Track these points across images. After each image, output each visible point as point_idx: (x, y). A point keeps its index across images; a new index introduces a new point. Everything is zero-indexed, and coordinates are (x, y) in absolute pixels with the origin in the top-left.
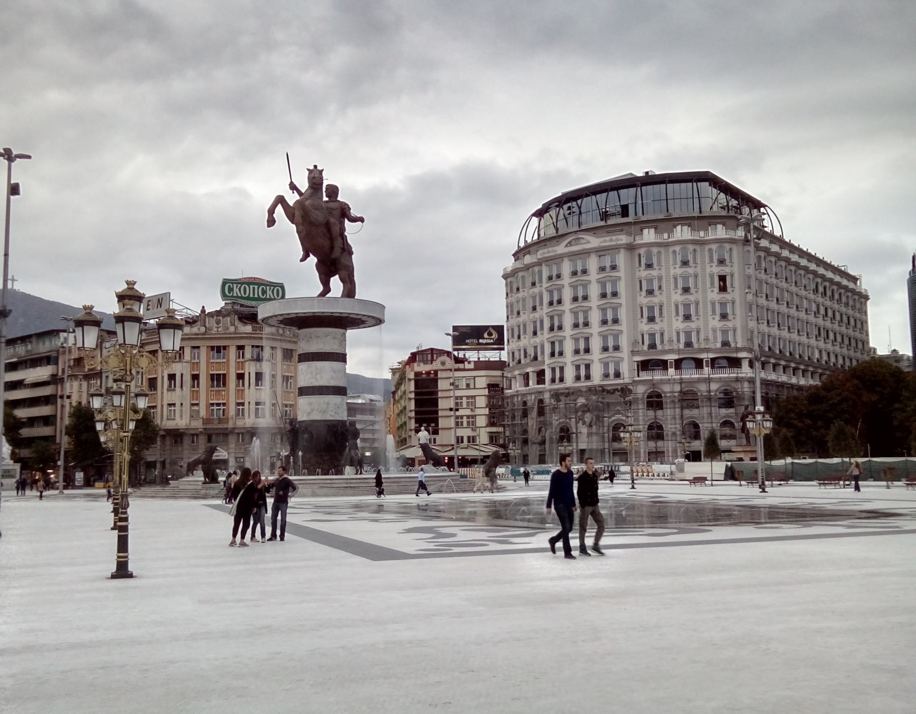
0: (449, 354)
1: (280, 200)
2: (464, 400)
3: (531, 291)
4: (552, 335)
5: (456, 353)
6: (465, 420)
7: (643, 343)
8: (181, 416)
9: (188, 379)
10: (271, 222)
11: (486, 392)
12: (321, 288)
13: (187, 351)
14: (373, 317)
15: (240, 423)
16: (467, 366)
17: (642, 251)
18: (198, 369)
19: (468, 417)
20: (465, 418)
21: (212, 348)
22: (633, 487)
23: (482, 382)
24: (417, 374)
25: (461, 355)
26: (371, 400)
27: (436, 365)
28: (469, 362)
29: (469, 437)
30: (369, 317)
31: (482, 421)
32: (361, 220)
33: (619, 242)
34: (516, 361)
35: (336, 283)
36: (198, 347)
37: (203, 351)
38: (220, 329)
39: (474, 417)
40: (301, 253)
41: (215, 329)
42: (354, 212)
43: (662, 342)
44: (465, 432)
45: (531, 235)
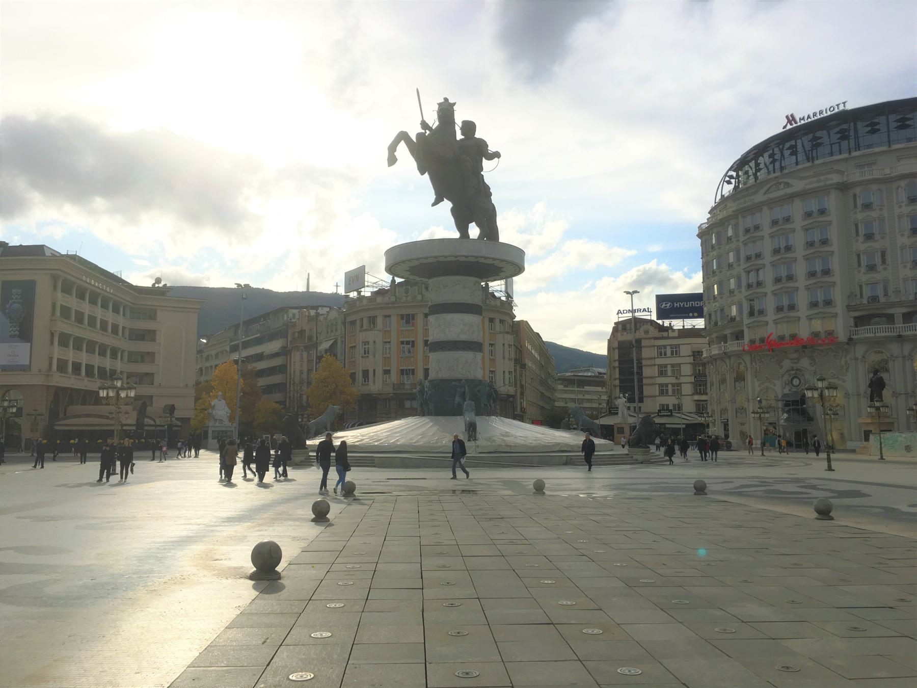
0: (652, 322)
1: (403, 136)
2: (669, 368)
3: (727, 247)
4: (750, 292)
5: (660, 322)
6: (670, 386)
7: (861, 296)
8: (374, 382)
10: (392, 160)
11: (691, 360)
12: (456, 235)
13: (380, 321)
16: (671, 334)
17: (858, 190)
19: (673, 385)
20: (670, 386)
21: (402, 316)
22: (830, 469)
23: (685, 350)
24: (620, 343)
25: (667, 323)
26: (600, 373)
27: (640, 334)
28: (674, 330)
29: (674, 405)
30: (503, 261)
31: (687, 389)
32: (497, 155)
33: (828, 182)
34: (713, 323)
35: (474, 231)
36: (389, 316)
37: (394, 319)
38: (409, 298)
39: (679, 385)
40: (432, 197)
41: (404, 298)
42: (492, 148)
43: (886, 295)
44: (670, 401)
45: (728, 189)
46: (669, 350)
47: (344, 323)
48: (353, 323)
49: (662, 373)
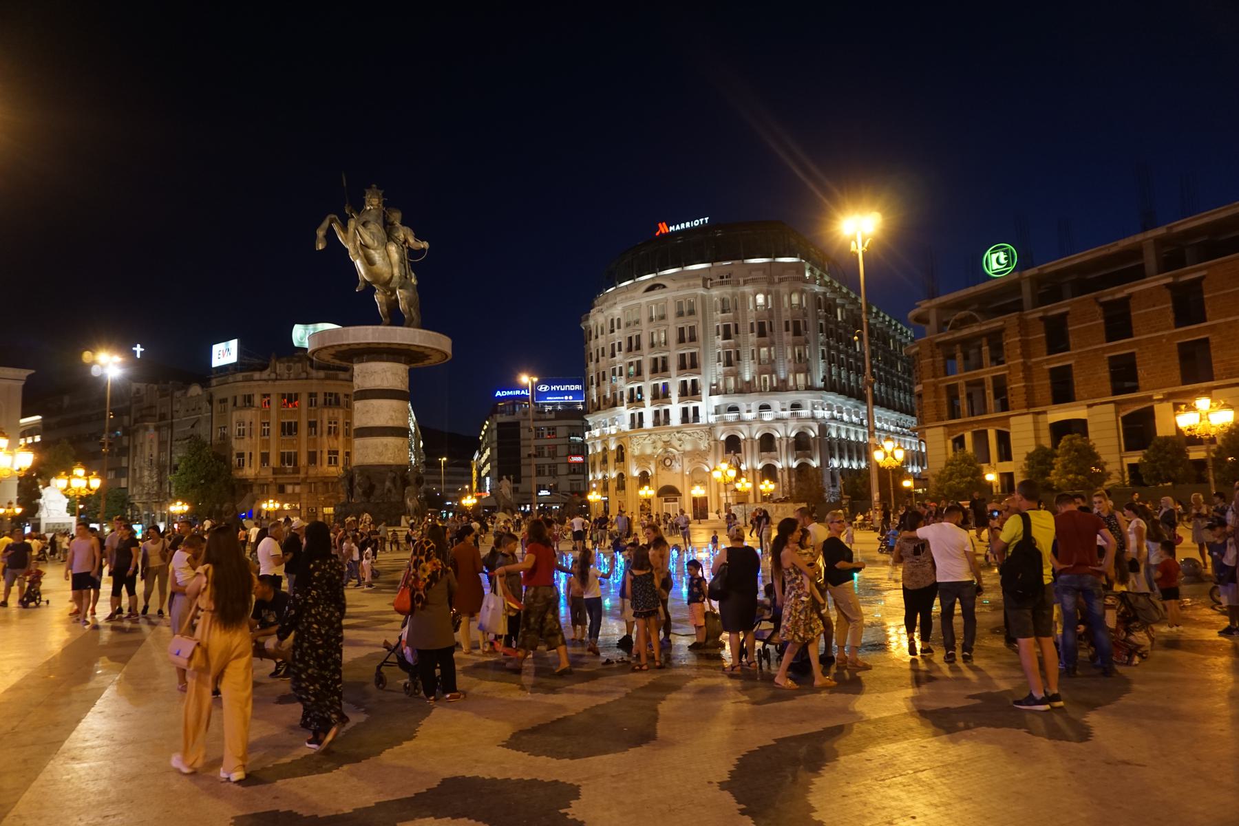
9: (257, 427)
13: (257, 400)
14: (438, 350)
15: (312, 472)
18: (268, 417)
21: (283, 396)
24: (499, 424)
30: (432, 349)
36: (269, 395)
37: (274, 400)
39: (556, 465)
46: (546, 432)
47: (211, 402)
48: (224, 401)
49: (539, 454)
